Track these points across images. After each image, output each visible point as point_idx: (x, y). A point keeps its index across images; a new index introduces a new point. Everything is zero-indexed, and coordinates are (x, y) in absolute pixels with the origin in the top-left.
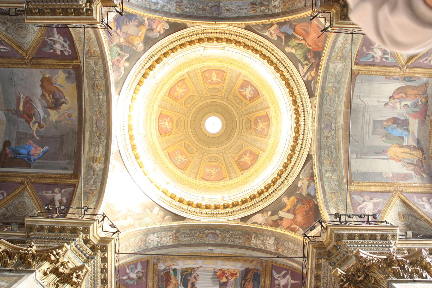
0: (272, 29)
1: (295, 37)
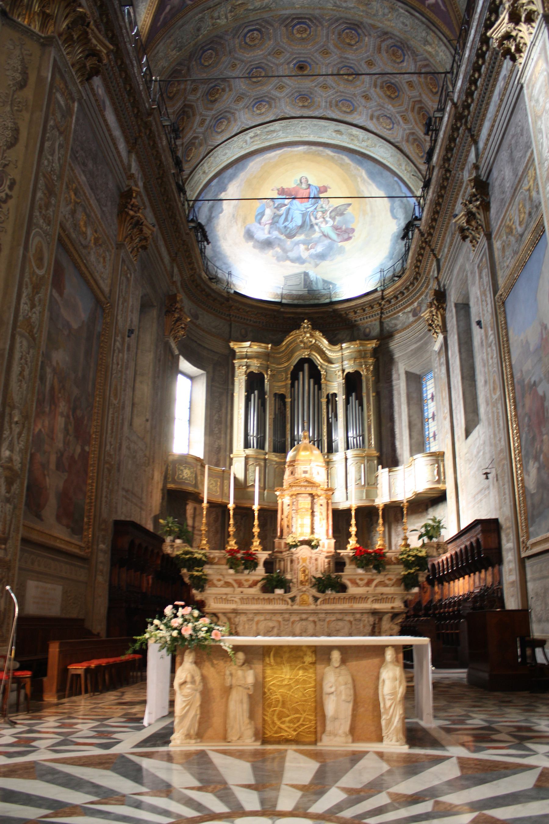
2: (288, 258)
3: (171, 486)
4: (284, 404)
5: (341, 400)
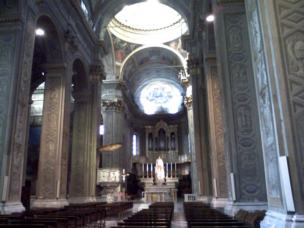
0: (133, 48)
1: (125, 50)
2: (157, 102)
3: (134, 162)
4: (157, 139)
5: (170, 138)
